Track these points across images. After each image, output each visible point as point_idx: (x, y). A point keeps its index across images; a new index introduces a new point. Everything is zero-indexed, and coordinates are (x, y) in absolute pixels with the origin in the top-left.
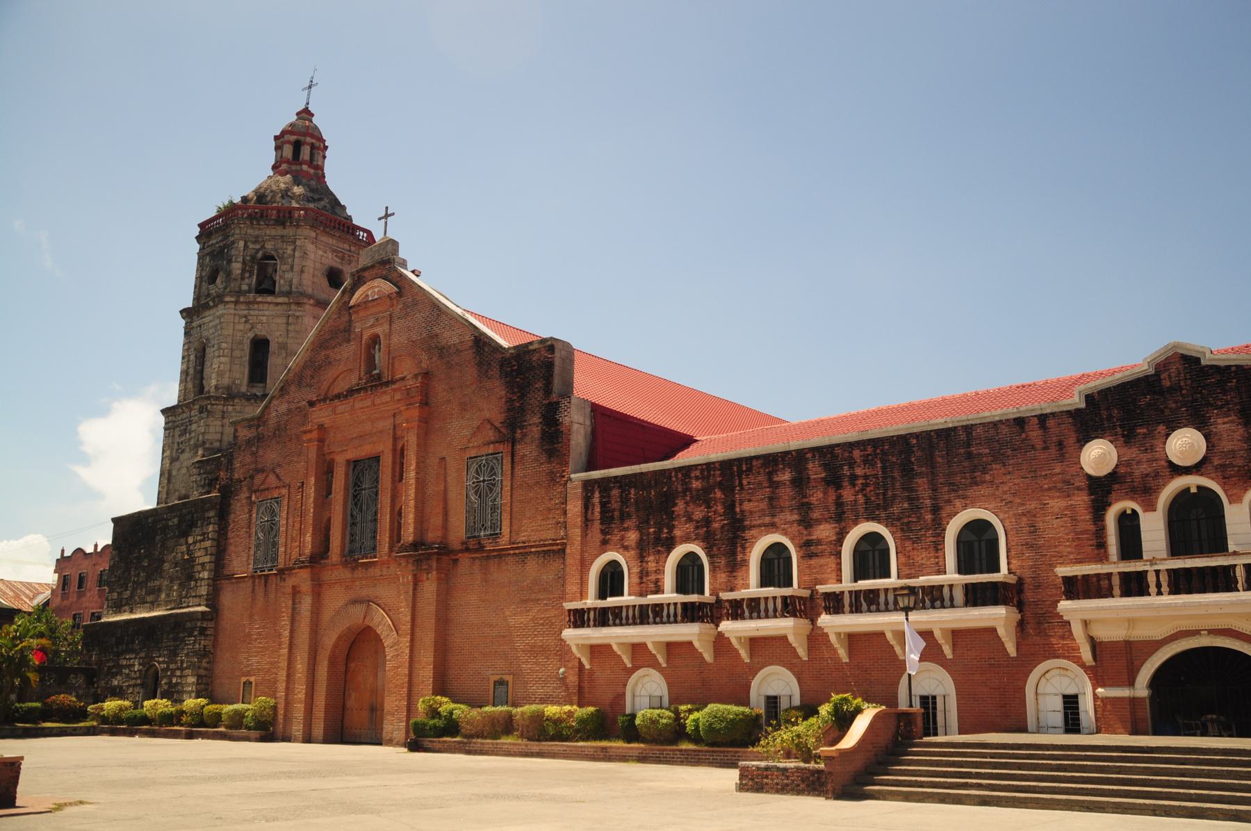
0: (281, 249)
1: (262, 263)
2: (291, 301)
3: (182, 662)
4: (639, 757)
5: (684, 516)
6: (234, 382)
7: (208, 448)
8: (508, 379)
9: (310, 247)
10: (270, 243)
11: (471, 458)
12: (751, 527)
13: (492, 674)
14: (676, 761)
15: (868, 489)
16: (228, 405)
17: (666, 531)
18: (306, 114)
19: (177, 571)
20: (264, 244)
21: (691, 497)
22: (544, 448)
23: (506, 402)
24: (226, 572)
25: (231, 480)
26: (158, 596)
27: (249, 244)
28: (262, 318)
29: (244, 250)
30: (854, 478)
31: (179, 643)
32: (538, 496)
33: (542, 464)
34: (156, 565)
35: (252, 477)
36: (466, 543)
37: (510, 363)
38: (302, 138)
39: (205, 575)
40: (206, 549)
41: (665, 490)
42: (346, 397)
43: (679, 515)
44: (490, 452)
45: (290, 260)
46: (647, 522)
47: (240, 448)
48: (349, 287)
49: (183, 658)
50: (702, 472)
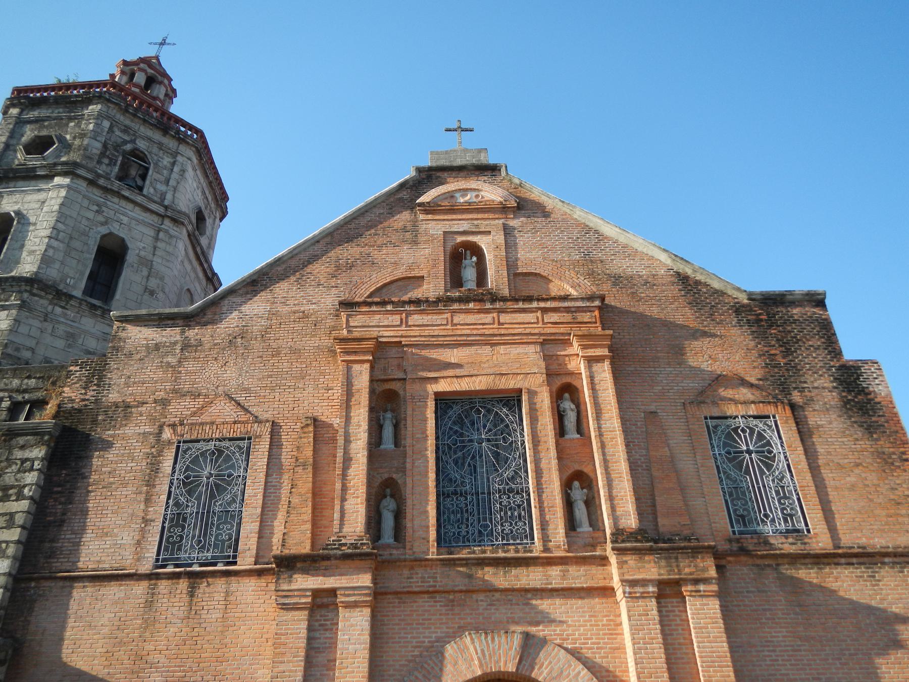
0: (156, 155)
1: (128, 159)
2: (169, 214)
6: (63, 280)
7: (9, 355)
8: (754, 329)
9: (190, 173)
10: (143, 142)
11: (712, 418)
16: (56, 305)
20: (135, 140)
22: (853, 419)
23: (760, 356)
24: (56, 565)
25: (97, 401)
27: (116, 129)
28: (122, 217)
29: (108, 133)
32: (867, 483)
33: (857, 440)
35: (164, 403)
36: (738, 541)
37: (751, 310)
38: (160, 78)
40: (12, 515)
44: (751, 413)
45: (165, 172)
48: (411, 183)
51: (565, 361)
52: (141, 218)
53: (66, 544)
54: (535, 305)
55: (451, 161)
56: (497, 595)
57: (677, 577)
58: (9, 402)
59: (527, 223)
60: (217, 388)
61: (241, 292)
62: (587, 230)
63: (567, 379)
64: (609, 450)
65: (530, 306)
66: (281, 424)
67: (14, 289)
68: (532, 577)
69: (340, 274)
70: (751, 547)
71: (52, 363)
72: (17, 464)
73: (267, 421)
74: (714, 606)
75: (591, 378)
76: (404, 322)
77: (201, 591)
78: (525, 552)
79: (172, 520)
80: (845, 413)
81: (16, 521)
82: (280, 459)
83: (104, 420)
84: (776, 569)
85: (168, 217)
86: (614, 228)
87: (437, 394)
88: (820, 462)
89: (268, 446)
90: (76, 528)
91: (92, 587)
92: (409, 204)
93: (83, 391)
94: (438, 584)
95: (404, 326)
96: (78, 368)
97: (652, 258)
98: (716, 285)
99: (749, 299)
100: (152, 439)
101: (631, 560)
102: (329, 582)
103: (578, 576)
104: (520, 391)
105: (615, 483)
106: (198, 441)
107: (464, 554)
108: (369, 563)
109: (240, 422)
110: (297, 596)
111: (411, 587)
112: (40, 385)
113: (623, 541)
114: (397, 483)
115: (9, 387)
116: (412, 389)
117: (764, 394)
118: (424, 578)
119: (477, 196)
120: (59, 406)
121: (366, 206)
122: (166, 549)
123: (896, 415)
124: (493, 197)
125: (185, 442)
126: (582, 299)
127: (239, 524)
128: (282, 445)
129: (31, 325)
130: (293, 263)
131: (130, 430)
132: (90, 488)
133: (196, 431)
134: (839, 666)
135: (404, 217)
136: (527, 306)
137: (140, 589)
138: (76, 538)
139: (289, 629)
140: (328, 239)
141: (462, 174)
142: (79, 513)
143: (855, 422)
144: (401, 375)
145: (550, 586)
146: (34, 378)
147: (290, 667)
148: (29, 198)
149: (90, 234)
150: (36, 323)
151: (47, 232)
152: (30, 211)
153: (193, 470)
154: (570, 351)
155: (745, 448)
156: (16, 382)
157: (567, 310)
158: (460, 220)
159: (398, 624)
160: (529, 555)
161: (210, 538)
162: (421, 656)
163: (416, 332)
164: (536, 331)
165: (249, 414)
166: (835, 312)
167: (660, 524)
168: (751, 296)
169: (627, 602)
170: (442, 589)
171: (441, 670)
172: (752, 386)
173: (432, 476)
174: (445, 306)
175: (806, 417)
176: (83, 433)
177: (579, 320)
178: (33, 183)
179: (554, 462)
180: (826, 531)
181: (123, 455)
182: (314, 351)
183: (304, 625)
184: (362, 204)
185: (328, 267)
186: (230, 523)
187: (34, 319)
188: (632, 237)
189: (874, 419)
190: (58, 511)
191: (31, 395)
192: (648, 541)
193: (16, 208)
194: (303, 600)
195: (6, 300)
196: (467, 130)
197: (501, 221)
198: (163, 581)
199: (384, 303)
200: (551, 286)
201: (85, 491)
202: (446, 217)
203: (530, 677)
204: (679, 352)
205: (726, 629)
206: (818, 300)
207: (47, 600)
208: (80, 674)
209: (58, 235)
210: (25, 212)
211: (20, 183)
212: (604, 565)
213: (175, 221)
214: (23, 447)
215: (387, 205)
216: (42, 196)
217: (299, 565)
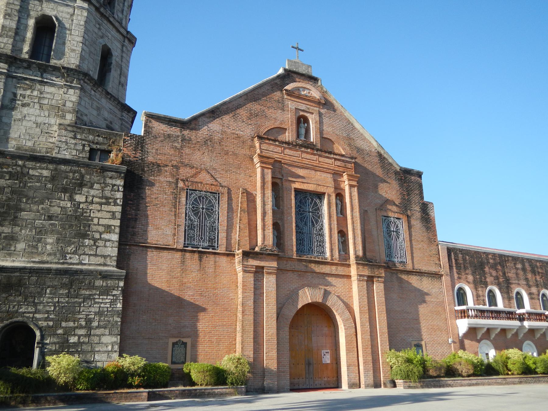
2: (128, 36)
3: (89, 321)
4: (518, 381)
5: (489, 273)
7: (79, 118)
11: (384, 216)
12: (512, 284)
13: (412, 341)
14: (532, 382)
15: (543, 278)
17: (483, 278)
19: (51, 224)
21: (490, 266)
23: (400, 194)
25: (142, 159)
26: (11, 245)
30: (539, 273)
31: (80, 300)
32: (424, 248)
35: (177, 167)
36: (387, 263)
39: (115, 237)
40: (114, 213)
41: (480, 260)
43: (487, 272)
44: (396, 217)
46: (475, 272)
47: (155, 137)
49: (93, 316)
50: (492, 256)
51: (340, 183)
52: (116, 36)
53: (140, 230)
54: (332, 156)
55: (296, 68)
56: (315, 274)
57: (373, 275)
58: (89, 148)
59: (327, 113)
60: (201, 164)
61: (207, 115)
62: (349, 122)
63: (339, 191)
64: (355, 225)
65: (330, 156)
66: (231, 189)
67: (75, 76)
68: (326, 269)
69: (252, 118)
70: (391, 266)
71: (93, 124)
72: (110, 187)
73: (226, 187)
74: (382, 285)
75: (351, 194)
76: (283, 152)
77: (204, 259)
78: (325, 259)
79: (188, 227)
80: (422, 221)
81: (117, 216)
82: (232, 206)
83: (148, 171)
84: (396, 274)
86: (360, 125)
87: (295, 188)
88: (413, 238)
89: (227, 199)
90: (144, 223)
91: (156, 252)
92: (280, 87)
93: (134, 152)
94: (296, 268)
95: (283, 154)
96: (129, 138)
97: (370, 142)
98: (390, 161)
99: (400, 170)
100: (173, 185)
101: (361, 267)
102: (262, 264)
103: (341, 270)
104: (325, 193)
105: (356, 238)
106: (196, 191)
107: (304, 258)
108: (276, 258)
109: (214, 185)
110: (250, 267)
111: (287, 268)
112: (105, 142)
113: (359, 261)
114: (279, 224)
115: (87, 139)
116: (286, 184)
117: (400, 210)
118: (291, 265)
119: (309, 93)
120: (123, 159)
121: (263, 83)
122: (188, 239)
123: (435, 224)
124: (315, 95)
125: (190, 190)
126: (349, 158)
127: (218, 233)
128: (232, 199)
129: (86, 101)
130: (230, 106)
131: (162, 179)
132: (147, 205)
133: (194, 186)
134: (409, 307)
135: (278, 94)
137: (178, 255)
138: (144, 228)
139: (247, 280)
140: (245, 97)
141: (302, 78)
142: (144, 216)
143: (424, 225)
144: (280, 177)
145: (332, 273)
146: (102, 137)
147: (249, 294)
148: (61, 8)
149: (97, 44)
150: (86, 99)
151: (80, 39)
152: (65, 19)
153: (196, 205)
155: (392, 230)
156: (91, 137)
157: (343, 161)
158: (301, 103)
159: (281, 281)
160: (326, 261)
161: (206, 237)
162: (290, 294)
163: (287, 158)
164: (332, 168)
165: (217, 182)
166: (425, 181)
167: (367, 255)
168: (401, 169)
169: (358, 282)
170: (297, 270)
171: (298, 300)
172: (397, 206)
173: (294, 225)
174: (299, 148)
175: (411, 221)
176: (138, 175)
177: (347, 167)
179: (336, 226)
180: (411, 263)
181: (160, 190)
182: (243, 156)
183: (252, 279)
184: (261, 82)
185: (246, 113)
186: (214, 232)
187: (86, 97)
188: (365, 132)
189: (429, 225)
190: (133, 213)
191: (101, 146)
192: (366, 262)
194: (252, 270)
196: (301, 50)
197: (317, 109)
198: (188, 253)
199: (275, 141)
200: (334, 146)
201: (144, 206)
202: (296, 100)
203: (325, 304)
204: (376, 187)
205: (385, 293)
206: (419, 175)
207: (136, 255)
208: (157, 289)
209: (85, 42)
210: (61, 19)
212: (349, 267)
213: (130, 40)
214: (111, 178)
215: (271, 85)
216: (71, 10)
217: (251, 255)
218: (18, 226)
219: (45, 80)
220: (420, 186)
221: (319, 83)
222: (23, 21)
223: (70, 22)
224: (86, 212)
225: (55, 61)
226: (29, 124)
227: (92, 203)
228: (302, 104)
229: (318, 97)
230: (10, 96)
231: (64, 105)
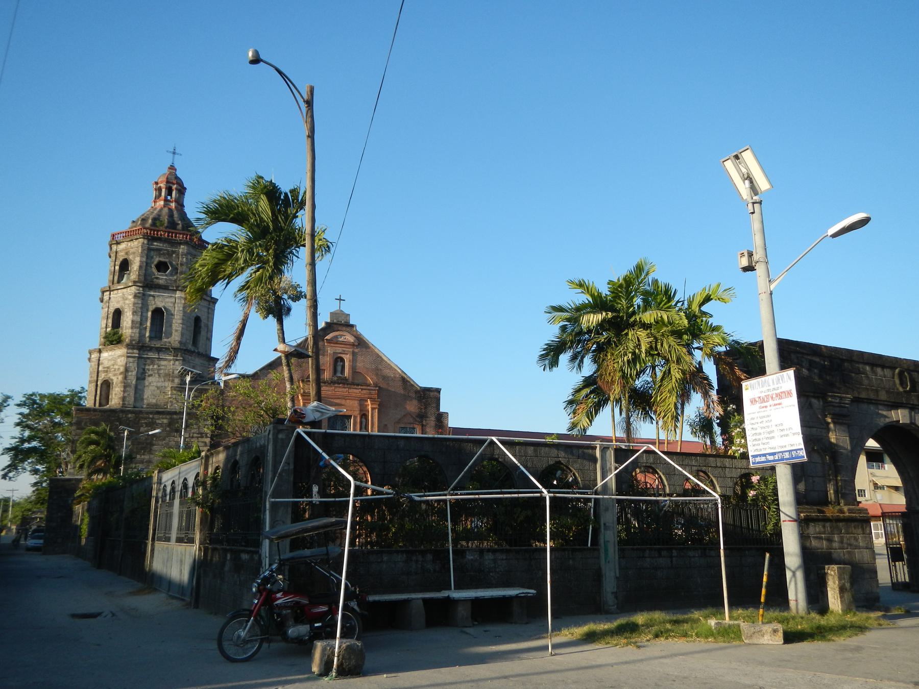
2: (213, 300)
18: (172, 168)
34: (143, 446)
38: (182, 189)
42: (330, 384)
54: (360, 387)
62: (378, 356)
85: (211, 301)
97: (396, 370)
98: (412, 383)
104: (350, 416)
119: (345, 338)
136: (357, 387)
148: (167, 300)
151: (180, 321)
154: (366, 403)
157: (369, 390)
178: (167, 291)
193: (163, 304)
195: (177, 356)
196: (343, 300)
197: (351, 350)
206: (438, 391)
211: (161, 290)
216: (173, 300)
218: (152, 454)
219: (161, 357)
220: (438, 400)
221: (355, 329)
222: (144, 314)
223: (174, 309)
224: (189, 444)
225: (165, 340)
226: (153, 388)
227: (193, 437)
228: (339, 348)
229: (352, 341)
230: (141, 371)
231: (173, 373)
